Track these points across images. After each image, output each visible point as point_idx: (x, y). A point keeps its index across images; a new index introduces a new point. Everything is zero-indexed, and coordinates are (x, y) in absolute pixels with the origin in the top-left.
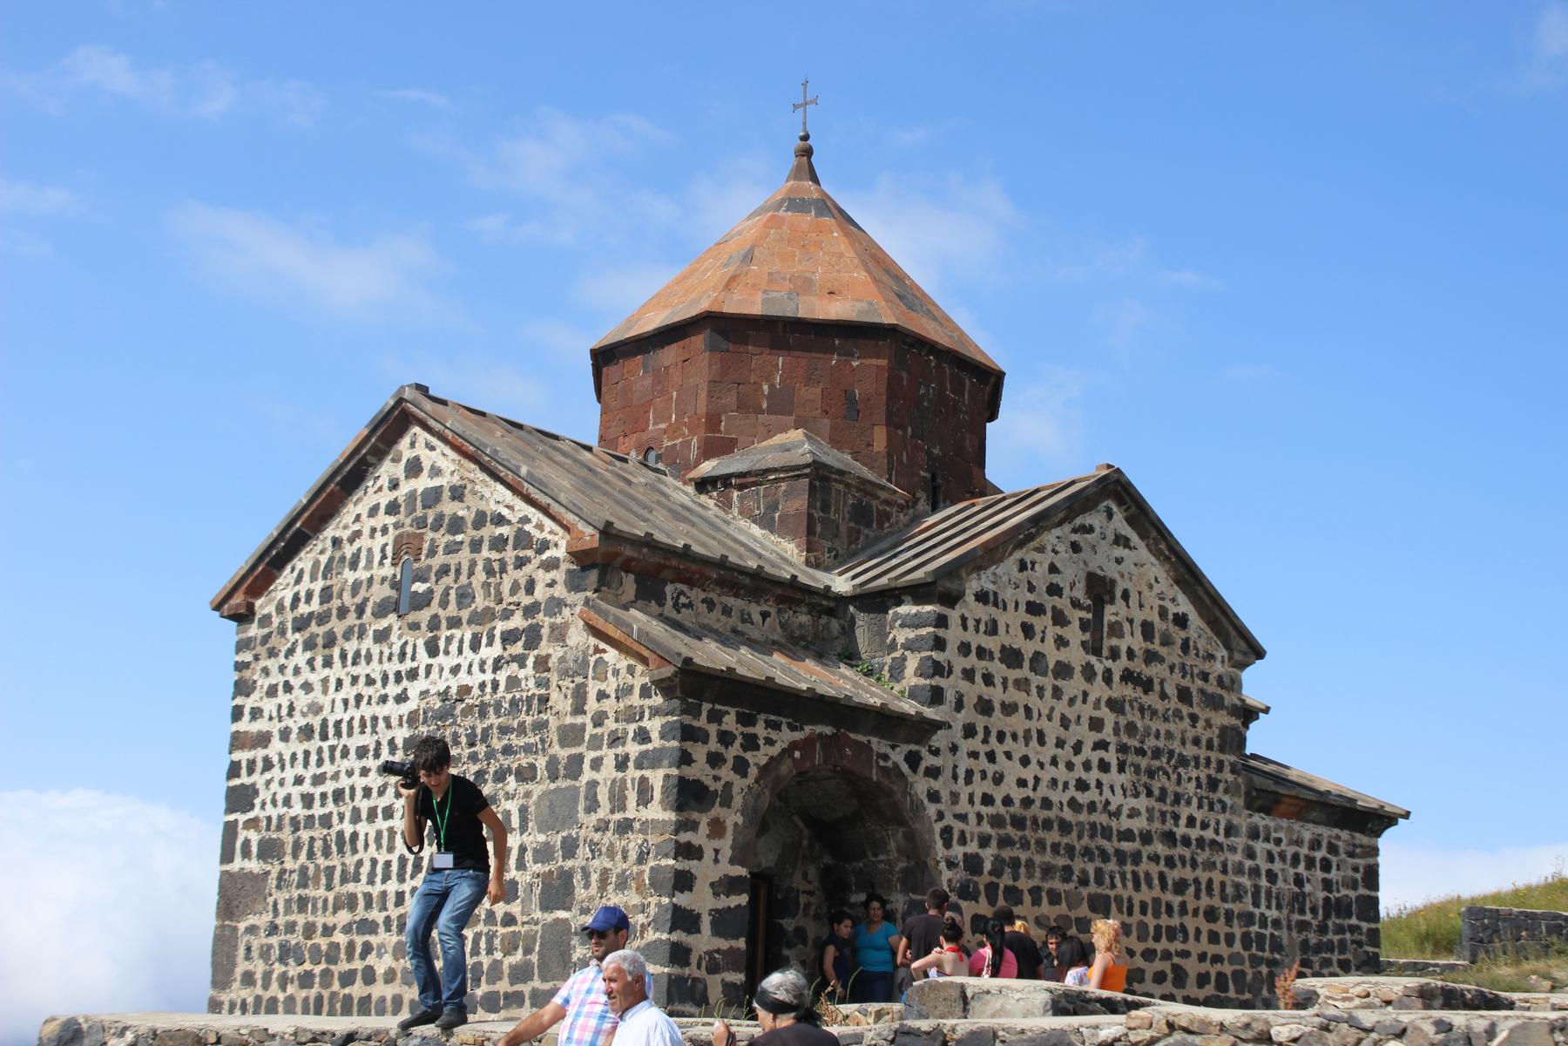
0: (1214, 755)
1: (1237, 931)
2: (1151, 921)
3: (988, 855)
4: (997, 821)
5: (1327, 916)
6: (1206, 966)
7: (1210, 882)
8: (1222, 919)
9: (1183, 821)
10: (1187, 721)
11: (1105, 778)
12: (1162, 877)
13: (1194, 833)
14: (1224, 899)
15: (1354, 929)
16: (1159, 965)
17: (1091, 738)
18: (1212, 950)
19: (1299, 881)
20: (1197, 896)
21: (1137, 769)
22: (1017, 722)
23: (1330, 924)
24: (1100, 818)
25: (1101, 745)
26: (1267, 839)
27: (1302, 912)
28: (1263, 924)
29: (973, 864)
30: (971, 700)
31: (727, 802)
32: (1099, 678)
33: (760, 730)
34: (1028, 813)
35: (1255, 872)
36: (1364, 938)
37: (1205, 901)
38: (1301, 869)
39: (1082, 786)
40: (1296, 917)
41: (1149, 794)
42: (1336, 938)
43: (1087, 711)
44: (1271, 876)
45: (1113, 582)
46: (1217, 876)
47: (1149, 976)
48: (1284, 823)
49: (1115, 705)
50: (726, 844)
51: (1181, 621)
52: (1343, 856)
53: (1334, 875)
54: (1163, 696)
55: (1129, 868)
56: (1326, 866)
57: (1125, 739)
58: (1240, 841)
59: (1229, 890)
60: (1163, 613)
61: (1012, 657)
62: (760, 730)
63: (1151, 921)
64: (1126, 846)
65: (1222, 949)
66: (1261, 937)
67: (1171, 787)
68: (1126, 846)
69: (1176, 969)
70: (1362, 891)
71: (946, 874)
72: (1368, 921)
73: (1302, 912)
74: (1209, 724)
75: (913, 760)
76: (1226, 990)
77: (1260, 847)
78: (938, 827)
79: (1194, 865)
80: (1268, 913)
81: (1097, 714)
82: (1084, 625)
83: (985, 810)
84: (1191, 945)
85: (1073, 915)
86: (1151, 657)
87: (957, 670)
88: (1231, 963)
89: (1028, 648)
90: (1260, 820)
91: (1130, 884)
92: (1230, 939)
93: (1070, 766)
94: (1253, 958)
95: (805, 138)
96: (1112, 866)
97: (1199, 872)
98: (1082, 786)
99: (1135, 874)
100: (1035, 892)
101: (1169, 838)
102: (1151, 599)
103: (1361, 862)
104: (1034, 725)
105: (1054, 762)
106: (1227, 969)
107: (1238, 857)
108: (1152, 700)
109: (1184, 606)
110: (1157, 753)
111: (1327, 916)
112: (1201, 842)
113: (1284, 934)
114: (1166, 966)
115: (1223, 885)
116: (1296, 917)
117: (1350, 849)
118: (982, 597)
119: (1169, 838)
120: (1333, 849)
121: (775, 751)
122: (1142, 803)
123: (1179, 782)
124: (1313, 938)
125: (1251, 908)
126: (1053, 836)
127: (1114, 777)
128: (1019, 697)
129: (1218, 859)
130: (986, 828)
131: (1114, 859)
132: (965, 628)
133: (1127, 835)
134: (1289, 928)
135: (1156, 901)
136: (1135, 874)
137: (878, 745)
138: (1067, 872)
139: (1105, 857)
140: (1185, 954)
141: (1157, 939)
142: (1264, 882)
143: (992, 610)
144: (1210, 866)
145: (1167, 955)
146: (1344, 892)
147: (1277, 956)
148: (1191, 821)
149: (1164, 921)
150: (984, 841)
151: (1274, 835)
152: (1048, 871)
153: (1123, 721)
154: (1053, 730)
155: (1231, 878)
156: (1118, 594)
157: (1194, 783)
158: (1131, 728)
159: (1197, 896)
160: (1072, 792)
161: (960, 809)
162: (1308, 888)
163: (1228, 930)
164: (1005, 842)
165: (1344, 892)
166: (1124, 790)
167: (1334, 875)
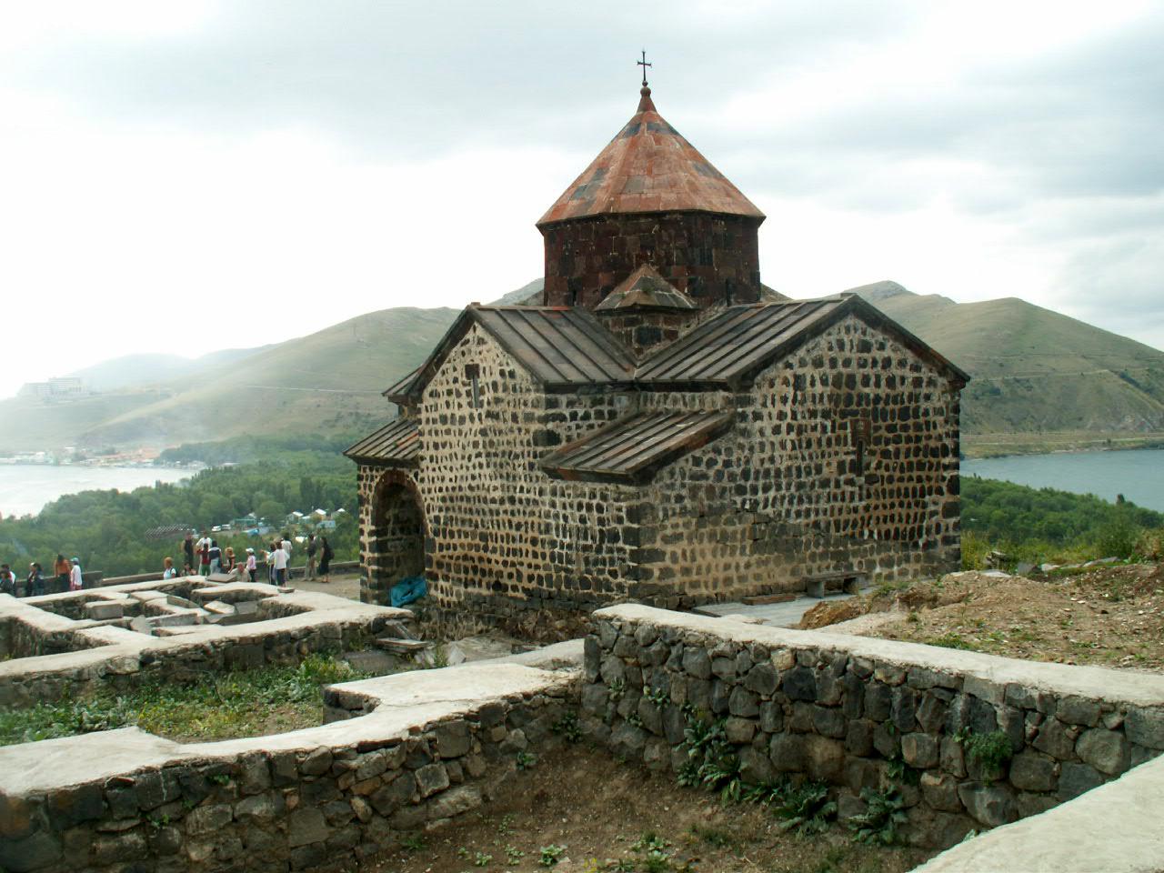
0: (532, 449)
1: (548, 551)
2: (505, 545)
3: (442, 515)
4: (444, 499)
5: (602, 541)
6: (531, 571)
7: (533, 523)
8: (540, 544)
9: (518, 490)
10: (517, 432)
11: (482, 472)
12: (510, 522)
13: (524, 496)
14: (541, 533)
15: (620, 550)
16: (510, 569)
17: (474, 452)
18: (534, 562)
19: (583, 520)
20: (526, 531)
21: (495, 465)
22: (447, 451)
23: (604, 546)
24: (483, 493)
25: (478, 455)
26: (563, 495)
27: (586, 538)
28: (562, 548)
29: (437, 519)
30: (431, 445)
31: (368, 503)
32: (477, 419)
33: (374, 473)
34: (454, 494)
35: (556, 516)
36: (627, 556)
37: (530, 534)
38: (584, 512)
39: (473, 477)
40: (582, 542)
41: (501, 476)
42: (607, 556)
43: (471, 438)
44: (565, 518)
45: (477, 366)
46: (536, 519)
47: (505, 574)
48: (571, 483)
49: (483, 432)
50: (370, 517)
51: (512, 374)
52: (611, 501)
53: (605, 515)
54: (505, 420)
55: (495, 518)
56: (600, 509)
57: (489, 449)
58: (547, 498)
59: (542, 528)
60: (502, 373)
61: (444, 419)
62: (374, 473)
63: (505, 545)
64: (494, 506)
65: (539, 561)
66: (560, 555)
67: (510, 469)
68: (494, 506)
69: (518, 571)
70: (627, 524)
71: (430, 526)
72: (631, 544)
73: (586, 538)
74: (527, 431)
75: (416, 475)
76: (542, 585)
77: (558, 500)
78: (426, 504)
79: (524, 513)
80: (564, 540)
81: (476, 439)
82: (468, 394)
83: (440, 495)
84: (523, 559)
85: (473, 542)
86: (498, 401)
87: (426, 431)
88: (545, 569)
89: (448, 413)
90: (559, 484)
91: (496, 527)
92: (544, 556)
93: (468, 468)
94: (556, 567)
95: (645, 84)
96: (488, 517)
97: (527, 517)
98: (473, 477)
99: (498, 521)
100: (459, 531)
101: (512, 500)
102: (497, 370)
103: (623, 504)
104: (453, 451)
105: (462, 468)
106: (543, 573)
107: (547, 508)
108: (502, 426)
109: (514, 366)
110: (504, 453)
111: (602, 541)
112: (528, 500)
113: (573, 554)
114: (513, 570)
115: (540, 525)
116: (582, 542)
117: (616, 496)
118: (431, 395)
119: (512, 500)
120: (604, 498)
121: (377, 480)
122: (498, 483)
123: (514, 469)
124: (592, 555)
125: (555, 538)
126: (464, 504)
127: (486, 471)
128: (446, 438)
129: (536, 510)
130: (440, 503)
131: (488, 513)
132: (427, 411)
133: (493, 501)
134: (577, 549)
135: (508, 535)
136: (498, 521)
137: (406, 471)
138: (470, 520)
139: (484, 513)
140: (522, 564)
141: (508, 555)
142: (561, 521)
143: (436, 399)
144: (533, 513)
145: (513, 564)
146: (614, 525)
147: (569, 566)
148: (522, 489)
149: (512, 545)
150: (440, 510)
151: (566, 492)
152: (463, 522)
153: (487, 440)
154: (459, 450)
155: (544, 520)
156: (481, 372)
157: (521, 468)
158: (492, 443)
159: (526, 531)
160: (470, 481)
161: (431, 495)
162: (589, 524)
163: (542, 550)
164: (447, 509)
165: (614, 525)
166: (490, 477)
167: (605, 515)
